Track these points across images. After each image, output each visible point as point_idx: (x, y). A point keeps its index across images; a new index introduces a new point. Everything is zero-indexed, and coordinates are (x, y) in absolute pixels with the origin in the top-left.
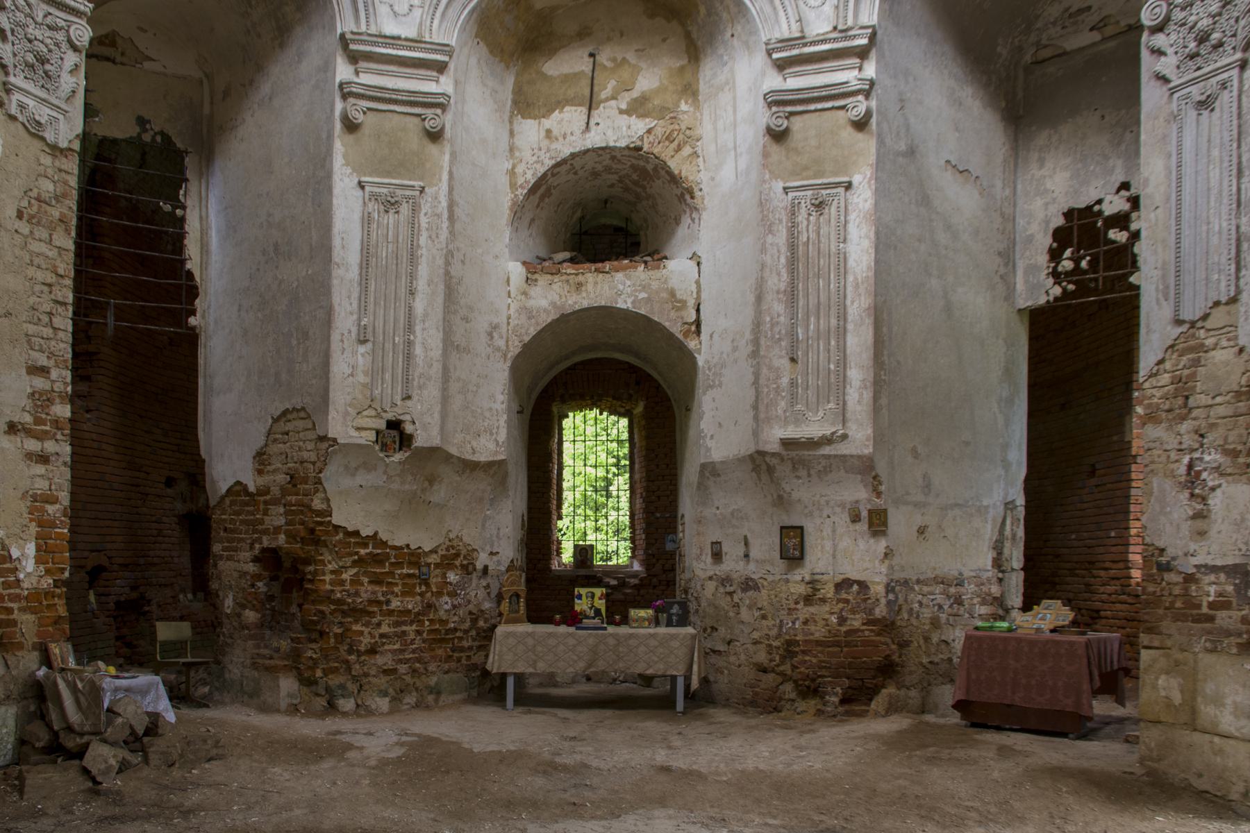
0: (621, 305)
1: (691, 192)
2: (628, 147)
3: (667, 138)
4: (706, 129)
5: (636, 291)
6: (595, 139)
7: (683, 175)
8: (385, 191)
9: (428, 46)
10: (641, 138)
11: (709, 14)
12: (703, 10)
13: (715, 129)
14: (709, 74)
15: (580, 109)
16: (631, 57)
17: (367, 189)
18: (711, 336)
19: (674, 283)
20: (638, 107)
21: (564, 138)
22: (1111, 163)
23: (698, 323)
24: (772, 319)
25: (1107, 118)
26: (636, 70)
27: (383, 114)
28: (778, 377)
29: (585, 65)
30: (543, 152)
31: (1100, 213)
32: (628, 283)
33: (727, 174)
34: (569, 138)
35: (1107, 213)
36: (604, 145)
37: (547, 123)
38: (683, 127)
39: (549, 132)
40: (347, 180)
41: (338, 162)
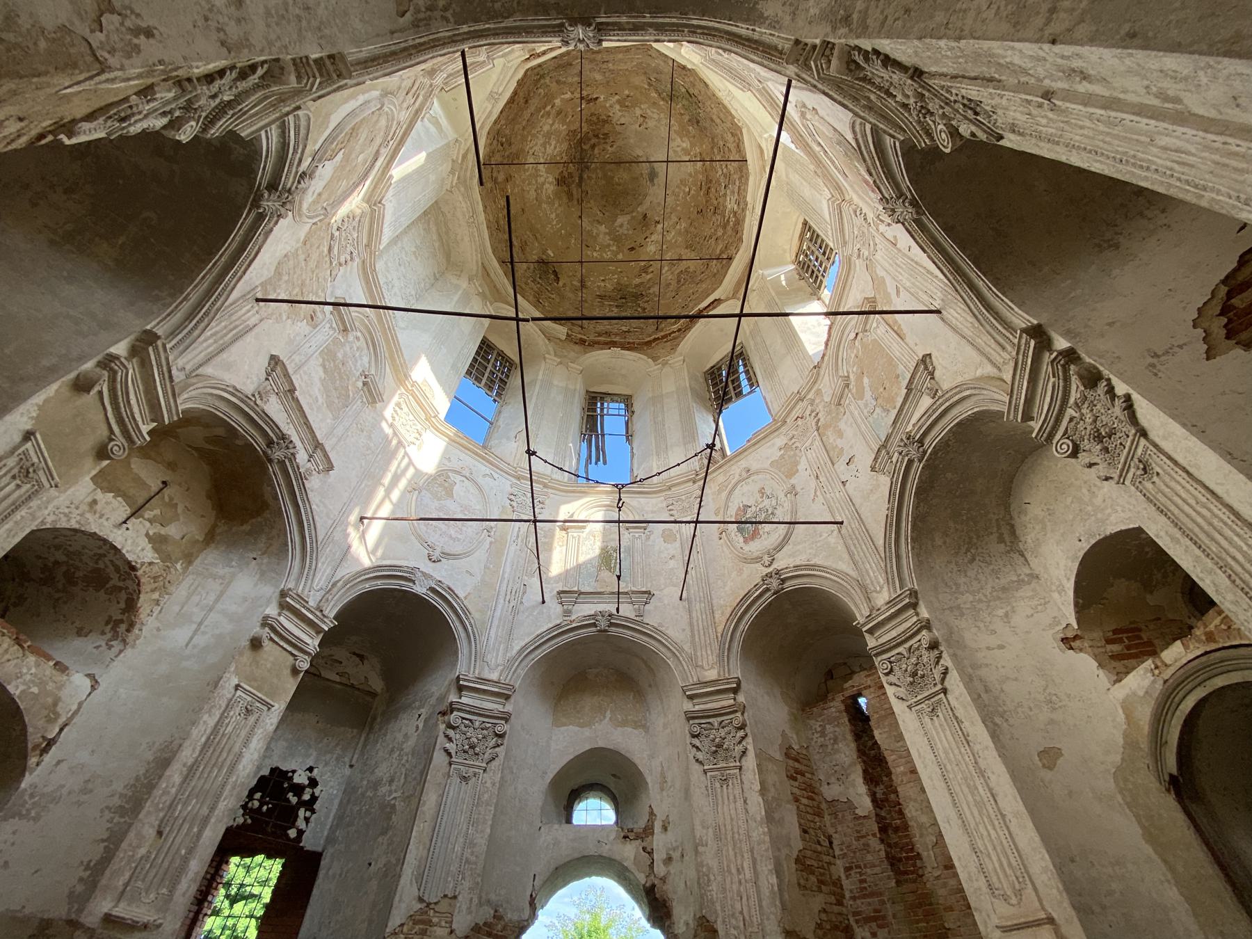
0: (11, 688)
1: (131, 626)
2: (129, 563)
3: (155, 578)
4: (180, 592)
5: (33, 682)
6: (118, 538)
7: (141, 610)
8: (35, 460)
9: (172, 404)
10: (142, 564)
11: (249, 533)
12: (246, 527)
13: (188, 598)
14: (210, 559)
15: (127, 508)
16: (180, 509)
17: (29, 445)
18: (59, 762)
19: (64, 694)
20: (158, 542)
21: (100, 517)
22: (311, 751)
23: (51, 743)
24: (167, 786)
25: (319, 724)
26: (175, 518)
27: (99, 404)
28: (139, 847)
29: (155, 485)
30: (78, 512)
31: (292, 778)
32: (33, 670)
33: (180, 635)
34: (103, 520)
35: (295, 781)
36: (119, 547)
37: (99, 495)
38: (168, 578)
39: (95, 502)
40: (25, 419)
41: (39, 398)
